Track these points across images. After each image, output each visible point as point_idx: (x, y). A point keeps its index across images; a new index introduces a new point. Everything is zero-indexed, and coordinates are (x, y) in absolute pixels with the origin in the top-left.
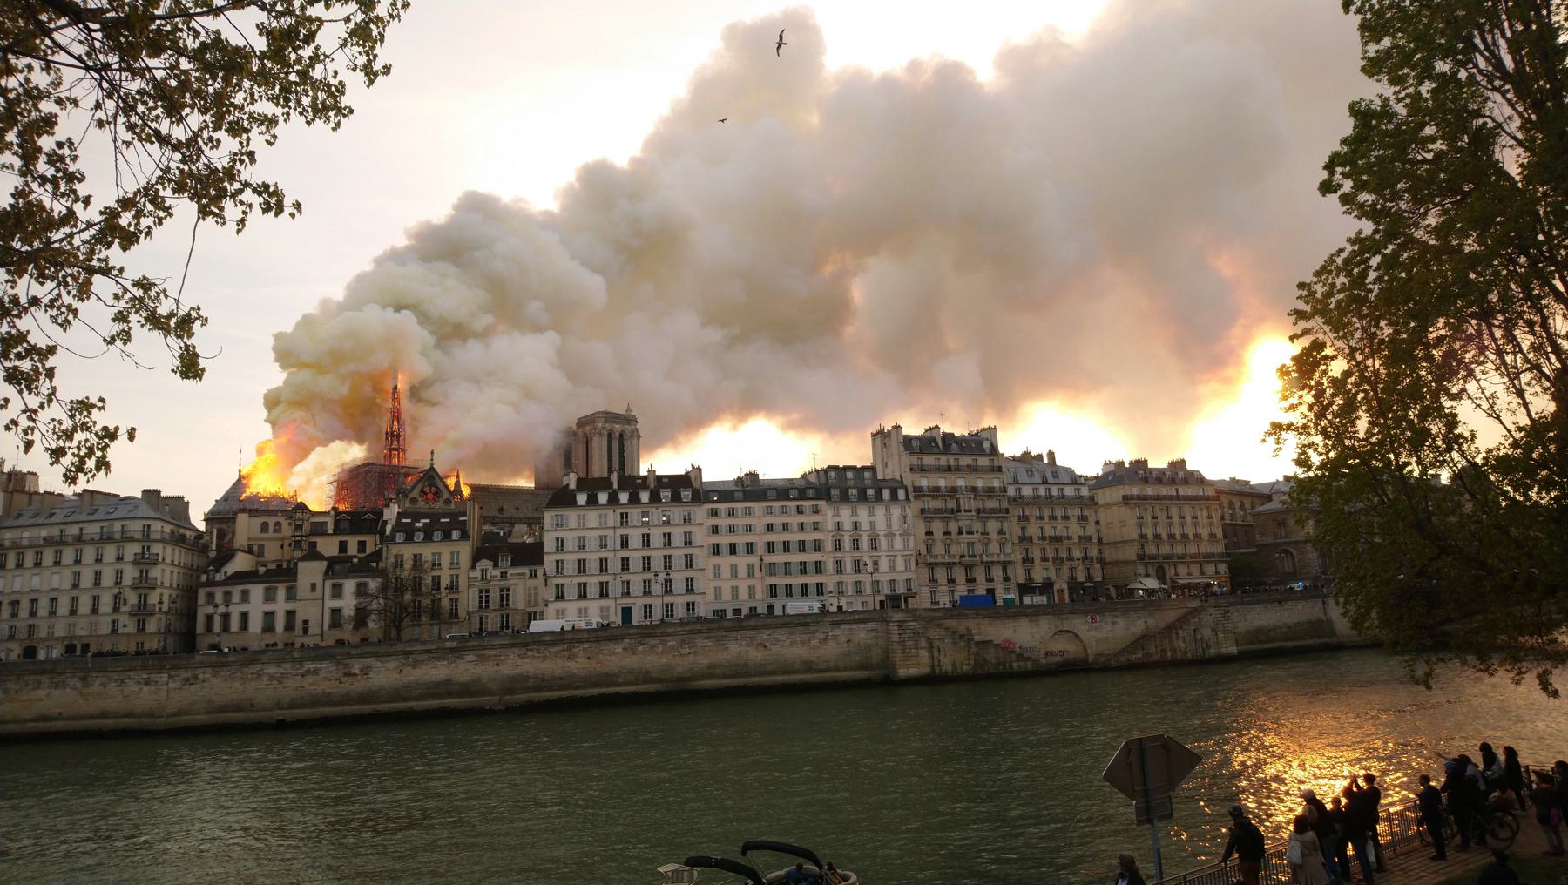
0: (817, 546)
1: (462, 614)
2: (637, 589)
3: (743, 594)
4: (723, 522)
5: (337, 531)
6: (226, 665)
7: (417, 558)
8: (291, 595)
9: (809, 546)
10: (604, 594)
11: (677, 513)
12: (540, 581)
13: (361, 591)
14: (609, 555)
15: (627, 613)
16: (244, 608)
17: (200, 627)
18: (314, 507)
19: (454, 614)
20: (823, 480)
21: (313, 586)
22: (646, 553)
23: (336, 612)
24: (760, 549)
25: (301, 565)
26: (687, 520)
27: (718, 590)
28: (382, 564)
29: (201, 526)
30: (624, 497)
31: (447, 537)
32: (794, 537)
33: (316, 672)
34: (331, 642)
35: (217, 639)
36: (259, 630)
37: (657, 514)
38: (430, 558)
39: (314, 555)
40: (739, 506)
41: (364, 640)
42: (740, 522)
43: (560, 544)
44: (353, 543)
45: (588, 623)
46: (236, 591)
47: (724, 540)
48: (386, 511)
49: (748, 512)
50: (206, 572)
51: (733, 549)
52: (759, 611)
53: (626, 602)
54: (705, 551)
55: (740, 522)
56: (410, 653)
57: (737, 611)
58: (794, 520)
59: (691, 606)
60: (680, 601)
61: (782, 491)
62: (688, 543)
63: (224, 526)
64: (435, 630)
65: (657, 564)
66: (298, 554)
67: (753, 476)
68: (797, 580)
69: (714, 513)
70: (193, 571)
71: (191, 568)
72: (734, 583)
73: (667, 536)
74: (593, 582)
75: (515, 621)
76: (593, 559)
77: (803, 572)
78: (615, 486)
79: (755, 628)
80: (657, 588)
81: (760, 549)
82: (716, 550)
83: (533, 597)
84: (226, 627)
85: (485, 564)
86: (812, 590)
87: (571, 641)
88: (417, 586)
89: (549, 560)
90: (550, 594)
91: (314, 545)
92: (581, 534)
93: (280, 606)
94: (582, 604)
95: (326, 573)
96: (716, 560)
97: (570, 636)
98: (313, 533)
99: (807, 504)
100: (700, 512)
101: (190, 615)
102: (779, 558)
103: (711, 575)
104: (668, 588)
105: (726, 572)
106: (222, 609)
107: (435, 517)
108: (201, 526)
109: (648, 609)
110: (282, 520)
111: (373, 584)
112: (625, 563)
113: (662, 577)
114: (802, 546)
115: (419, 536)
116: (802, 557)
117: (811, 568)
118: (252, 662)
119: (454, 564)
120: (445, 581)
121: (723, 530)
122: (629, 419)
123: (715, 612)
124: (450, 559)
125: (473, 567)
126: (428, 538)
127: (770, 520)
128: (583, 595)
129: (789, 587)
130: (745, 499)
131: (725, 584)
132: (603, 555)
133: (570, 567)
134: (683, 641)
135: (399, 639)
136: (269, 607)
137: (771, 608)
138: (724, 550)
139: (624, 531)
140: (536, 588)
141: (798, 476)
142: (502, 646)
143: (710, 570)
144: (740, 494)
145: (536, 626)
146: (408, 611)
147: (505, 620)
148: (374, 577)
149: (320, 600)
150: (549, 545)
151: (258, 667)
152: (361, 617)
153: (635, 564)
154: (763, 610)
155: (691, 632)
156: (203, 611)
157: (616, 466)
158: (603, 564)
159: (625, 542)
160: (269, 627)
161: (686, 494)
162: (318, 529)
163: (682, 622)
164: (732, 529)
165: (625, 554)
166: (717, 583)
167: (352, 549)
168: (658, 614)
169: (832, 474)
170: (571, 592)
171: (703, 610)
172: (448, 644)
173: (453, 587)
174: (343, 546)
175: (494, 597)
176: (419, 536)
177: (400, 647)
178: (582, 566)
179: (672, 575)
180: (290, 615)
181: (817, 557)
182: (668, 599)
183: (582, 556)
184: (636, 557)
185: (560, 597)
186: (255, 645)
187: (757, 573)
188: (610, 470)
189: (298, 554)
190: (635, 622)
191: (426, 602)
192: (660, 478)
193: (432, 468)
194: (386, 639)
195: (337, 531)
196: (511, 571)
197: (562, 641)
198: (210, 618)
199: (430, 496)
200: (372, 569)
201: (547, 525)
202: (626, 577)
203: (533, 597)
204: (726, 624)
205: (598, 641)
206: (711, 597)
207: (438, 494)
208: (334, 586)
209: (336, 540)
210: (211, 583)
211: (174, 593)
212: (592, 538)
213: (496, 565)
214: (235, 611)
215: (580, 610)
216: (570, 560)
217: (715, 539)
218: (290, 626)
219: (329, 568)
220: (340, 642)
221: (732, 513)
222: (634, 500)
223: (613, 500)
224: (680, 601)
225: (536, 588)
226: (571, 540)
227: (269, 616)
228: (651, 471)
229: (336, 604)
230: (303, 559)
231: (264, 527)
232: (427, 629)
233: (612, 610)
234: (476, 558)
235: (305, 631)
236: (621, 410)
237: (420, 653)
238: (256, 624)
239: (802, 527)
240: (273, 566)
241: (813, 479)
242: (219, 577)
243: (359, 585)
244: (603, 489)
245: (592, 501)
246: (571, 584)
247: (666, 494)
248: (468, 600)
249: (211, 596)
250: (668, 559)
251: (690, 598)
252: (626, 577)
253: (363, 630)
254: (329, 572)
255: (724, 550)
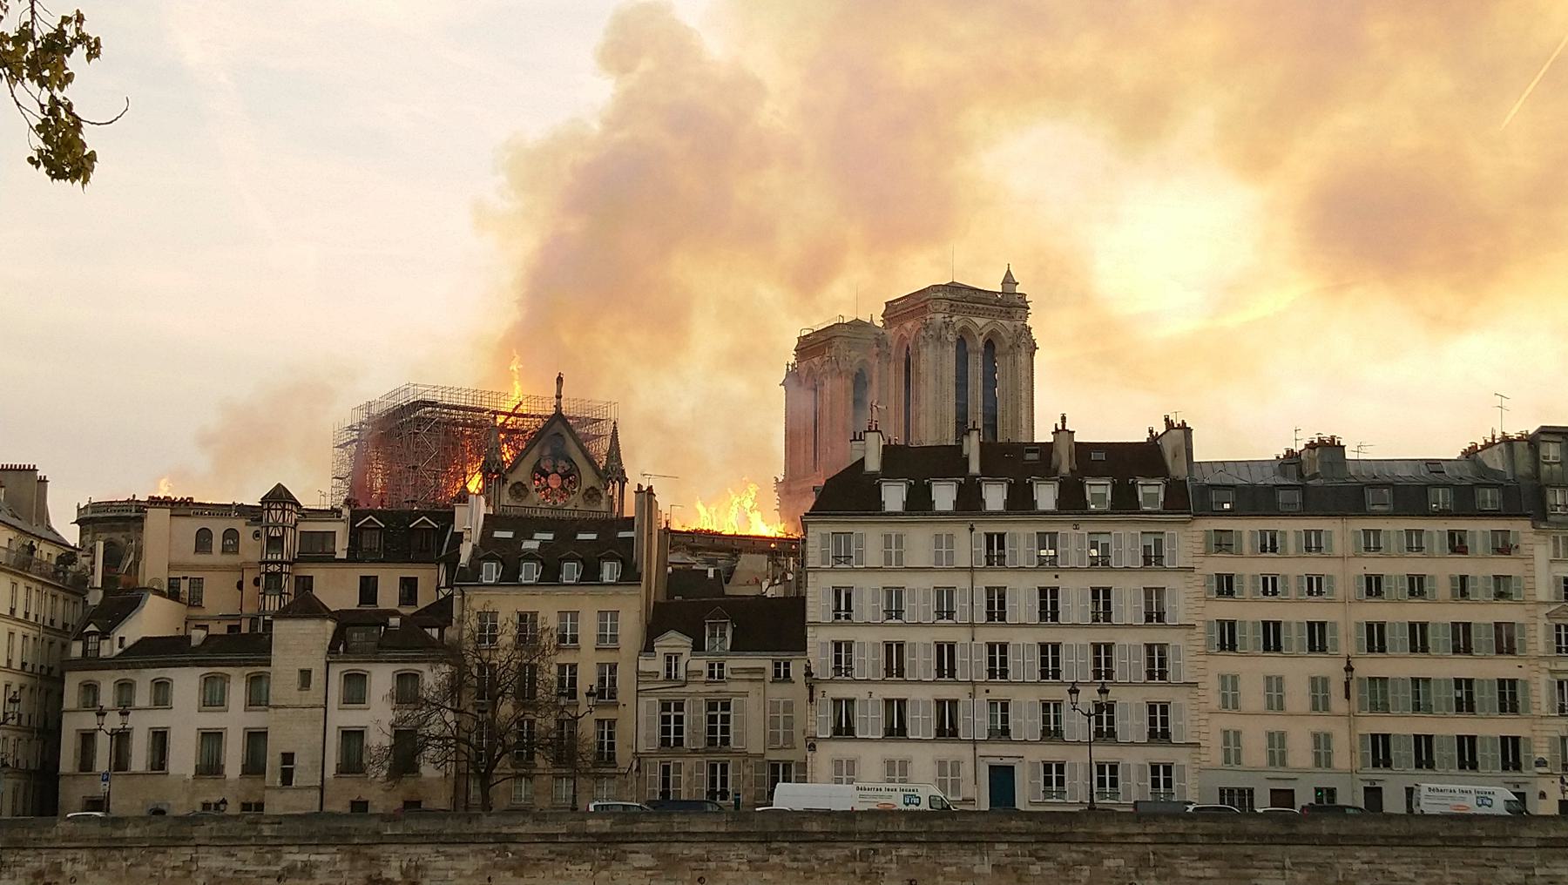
0: (1505, 641)
1: (623, 755)
2: (1026, 721)
3: (1300, 754)
4: (1248, 567)
5: (354, 557)
6: (119, 845)
7: (526, 621)
8: (257, 698)
9: (1480, 638)
10: (947, 729)
11: (1127, 538)
12: (798, 690)
13: (406, 690)
14: (960, 636)
15: (1002, 778)
16: (159, 719)
17: (68, 760)
18: (306, 503)
19: (606, 755)
20: (1524, 465)
21: (306, 675)
22: (1049, 635)
23: (352, 737)
24: (1347, 640)
25: (281, 628)
26: (1153, 558)
27: (1232, 740)
28: (450, 633)
29: (71, 535)
30: (995, 496)
31: (591, 575)
32: (1440, 613)
33: (307, 871)
34: (339, 806)
35: (101, 788)
36: (190, 772)
37: (1074, 539)
38: (553, 623)
39: (306, 606)
40: (1292, 528)
41: (412, 805)
42: (1292, 568)
43: (843, 603)
44: (389, 581)
45: (910, 798)
46: (144, 680)
47: (1249, 612)
48: (460, 511)
49: (1313, 544)
50: (82, 636)
51: (1272, 638)
52: (1341, 800)
53: (1000, 752)
54: (1199, 639)
55: (1292, 568)
56: (510, 839)
57: (1283, 797)
58: (1441, 569)
59: (1162, 774)
60: (1134, 760)
61: (1413, 491)
62: (1155, 616)
63: (118, 537)
64: (565, 789)
65: (1076, 664)
66: (272, 603)
67: (1329, 449)
68: (1447, 727)
69: (1223, 544)
70: (55, 634)
71: (50, 628)
72: (1275, 723)
73: (1102, 597)
74: (921, 697)
75: (740, 780)
76: (921, 642)
77: (1466, 705)
78: (974, 468)
79: (1332, 841)
80: (1076, 724)
81: (1347, 640)
82: (1227, 636)
83: (781, 724)
84: (120, 761)
85: (675, 641)
86: (1488, 754)
87: (871, 837)
88: (526, 692)
89: (819, 641)
90: (821, 721)
91: (305, 584)
92: (894, 580)
93: (235, 720)
94: (896, 750)
95: (333, 648)
96: (1229, 663)
97: (866, 825)
98: (304, 558)
99: (1478, 529)
100: (1187, 540)
101: (47, 732)
102: (1399, 666)
103: (1215, 702)
104: (1104, 725)
105: (1252, 695)
106: (113, 721)
107: (564, 528)
108: (71, 535)
109: (1054, 774)
110: (239, 524)
111: (433, 677)
112: (998, 658)
113: (1089, 696)
114: (1462, 639)
115: (530, 572)
116: (1464, 667)
117: (1486, 697)
118: (177, 841)
119: (607, 639)
120: (587, 679)
121: (1247, 588)
122: (1010, 303)
123: (1226, 793)
124: (596, 625)
125: (648, 648)
126: (551, 576)
127: (1374, 566)
128: (896, 731)
129: (1424, 749)
130: (1305, 511)
131: (1250, 724)
132: (945, 635)
133: (868, 661)
134: (1143, 861)
135: (487, 806)
136: (212, 721)
137: (1374, 794)
138: (1250, 637)
139: (995, 579)
140: (789, 706)
141: (1456, 455)
142: (712, 838)
143: (1212, 686)
144: (1297, 496)
145: (788, 796)
146: (504, 740)
147: (717, 772)
148: (436, 661)
149: (321, 709)
150: (818, 606)
151: (186, 853)
152: (406, 751)
153: (1023, 662)
154: (1350, 796)
155: (1162, 839)
156: (74, 724)
157: (976, 416)
158: (945, 658)
159: (997, 607)
160: (210, 767)
161: (1150, 491)
162: (317, 550)
163: (1140, 813)
164: (1270, 586)
165: (996, 635)
166: (1230, 722)
167: (388, 596)
168: (1077, 790)
169: (1552, 451)
170: (870, 720)
171: (1193, 790)
172: (593, 825)
173: (605, 692)
174: (368, 589)
175: (694, 719)
176: (530, 572)
177: (487, 824)
178: (894, 661)
179: (1114, 694)
180: (256, 739)
181: (1505, 668)
182: (1104, 753)
183: (895, 635)
184: (1024, 641)
185: (844, 730)
186: (180, 805)
187: (1338, 703)
188: (962, 429)
189: (272, 603)
190: (1021, 803)
191: (545, 723)
192: (1084, 449)
193: (558, 416)
194: (460, 806)
195: (354, 557)
196: (732, 663)
197: (848, 836)
198: (87, 738)
199: (554, 482)
200: (429, 644)
201: (813, 559)
202: (999, 692)
203: (781, 724)
204: (1253, 826)
205: (933, 842)
206: (1215, 755)
207: (570, 475)
208: (349, 678)
209: (352, 576)
210: (92, 662)
211: (16, 681)
212: (919, 588)
213: (698, 647)
214: (141, 725)
215: (890, 764)
216: (868, 641)
217: (1226, 610)
218: (253, 767)
219: (339, 637)
220: (359, 807)
221: (1270, 545)
222: (1020, 502)
223: (969, 502)
224: (1134, 760)
225: (789, 706)
226: (868, 590)
227: (212, 739)
228: (1061, 432)
229: (353, 718)
230: (284, 614)
231: (203, 540)
232: (545, 787)
233: (967, 769)
234: (655, 627)
235: (287, 777)
236: (992, 283)
237: (531, 839)
238: (183, 757)
239: (1462, 587)
240: (219, 629)
241: (1495, 461)
242: (109, 649)
243: (401, 677)
244: (944, 475)
245: (919, 503)
246: (870, 698)
247: (1098, 490)
248: (638, 725)
249: (91, 689)
250: (1103, 655)
251: (1160, 754)
252: (999, 692)
253: (409, 781)
254: (338, 647)
255: (1250, 637)
